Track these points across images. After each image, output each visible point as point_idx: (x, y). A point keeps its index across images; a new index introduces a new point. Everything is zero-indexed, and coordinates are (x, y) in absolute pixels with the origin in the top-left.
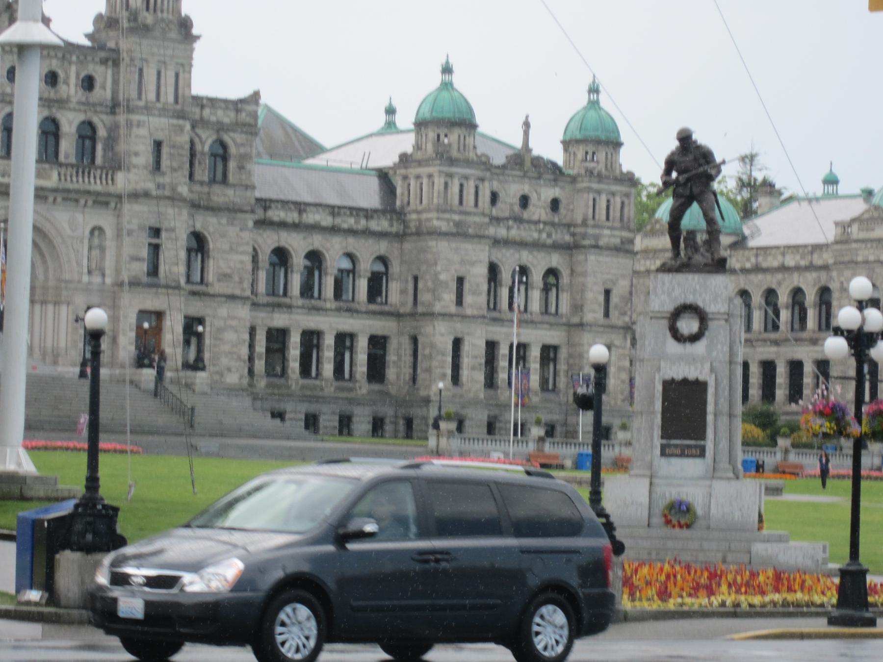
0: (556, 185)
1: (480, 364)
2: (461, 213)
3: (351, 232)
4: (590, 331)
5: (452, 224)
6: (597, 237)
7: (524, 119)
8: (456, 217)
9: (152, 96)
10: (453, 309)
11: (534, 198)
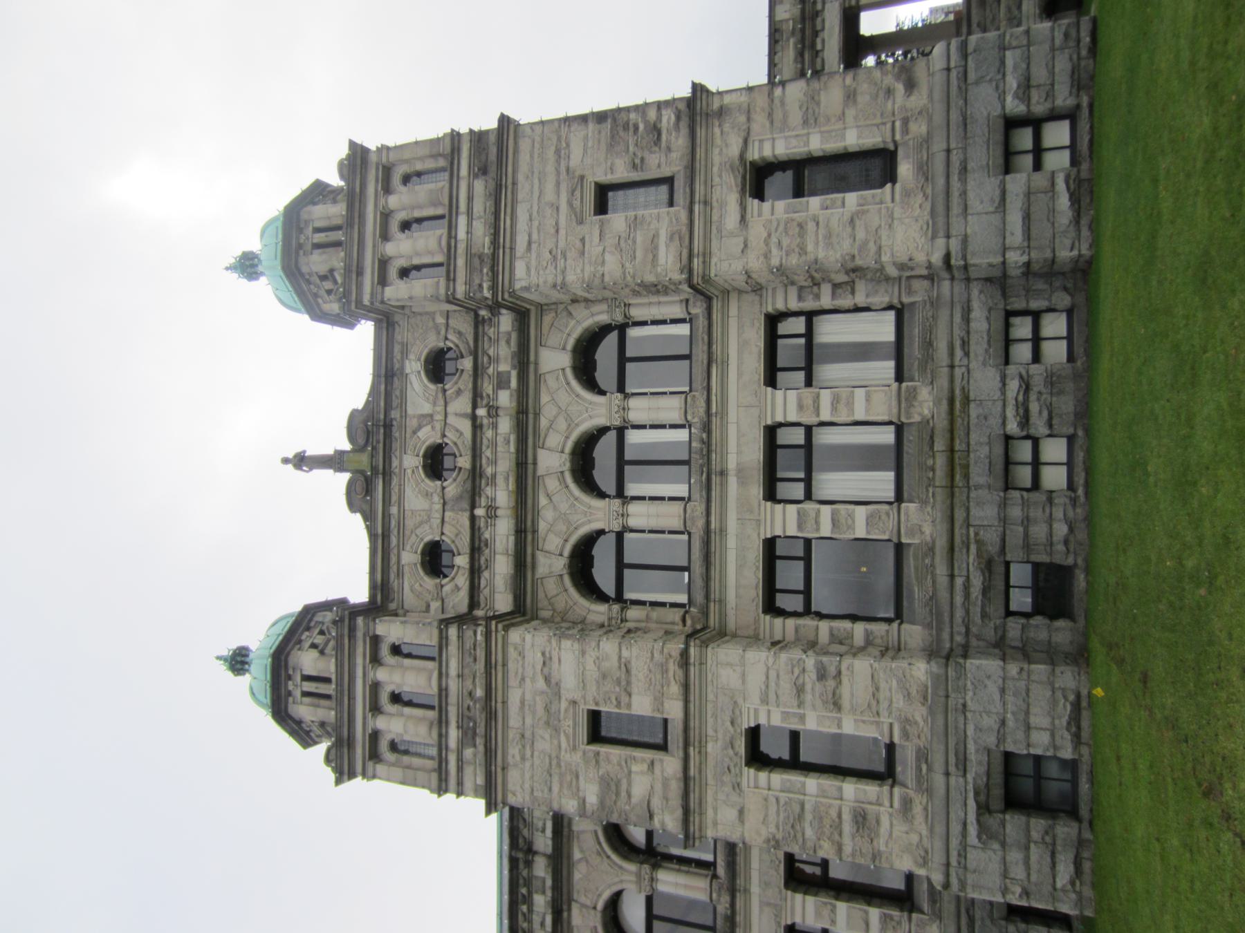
0: (402, 368)
1: (822, 675)
4: (706, 255)
5: (468, 753)
7: (290, 466)
8: (453, 734)
10: (670, 764)
11: (428, 436)
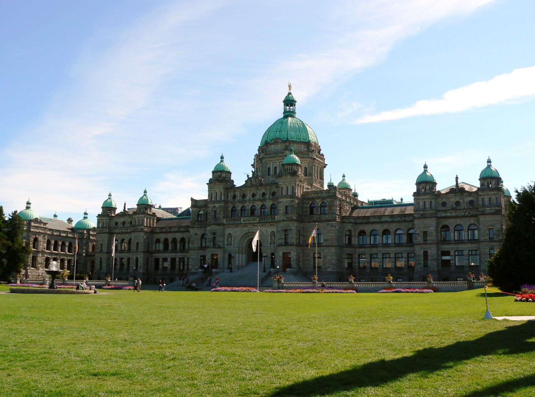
1: (435, 259)
2: (423, 210)
3: (398, 222)
6: (484, 211)
9: (284, 193)
11: (461, 201)
